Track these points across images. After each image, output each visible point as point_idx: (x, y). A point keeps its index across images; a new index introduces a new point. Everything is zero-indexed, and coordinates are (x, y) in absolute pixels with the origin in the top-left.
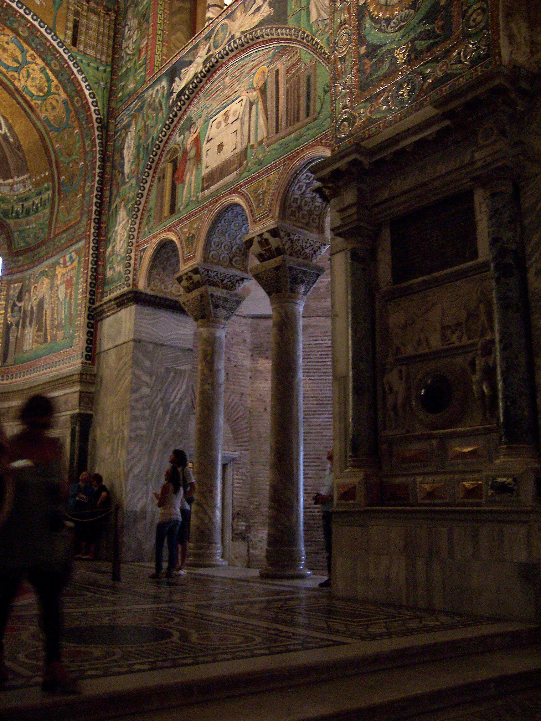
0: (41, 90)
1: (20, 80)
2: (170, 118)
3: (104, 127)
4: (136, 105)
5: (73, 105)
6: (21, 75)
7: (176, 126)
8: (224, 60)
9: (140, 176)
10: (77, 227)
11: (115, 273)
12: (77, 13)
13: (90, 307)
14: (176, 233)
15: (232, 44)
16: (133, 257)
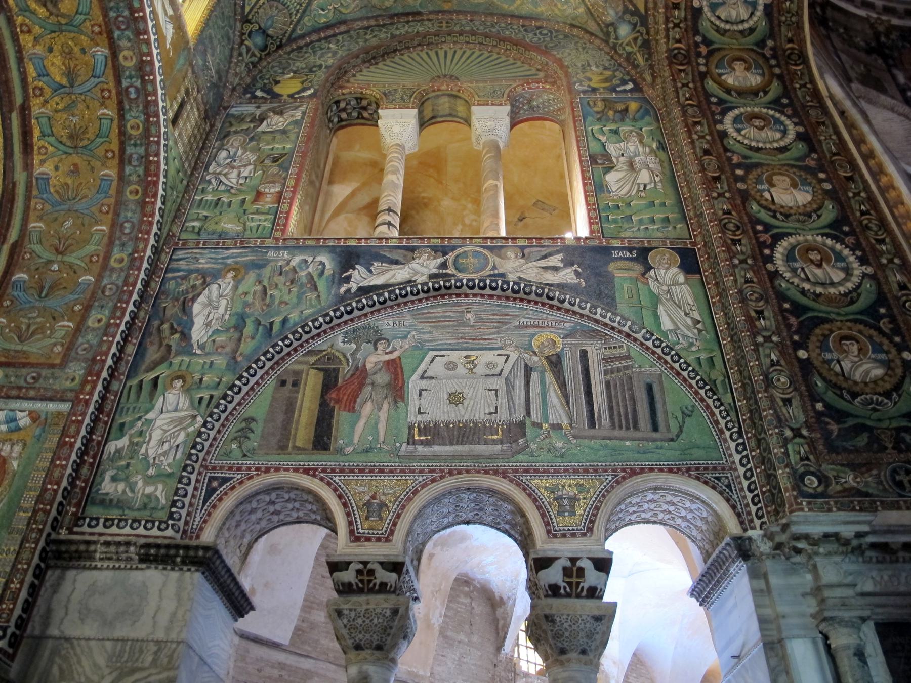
0: (71, 137)
1: (46, 102)
2: (338, 309)
3: (157, 251)
4: (240, 255)
5: (120, 192)
6: (57, 99)
7: (339, 325)
8: (469, 291)
9: (239, 359)
10: (44, 372)
11: (133, 491)
12: (187, 92)
13: (49, 535)
14: (329, 484)
15: (500, 282)
16: (193, 482)
